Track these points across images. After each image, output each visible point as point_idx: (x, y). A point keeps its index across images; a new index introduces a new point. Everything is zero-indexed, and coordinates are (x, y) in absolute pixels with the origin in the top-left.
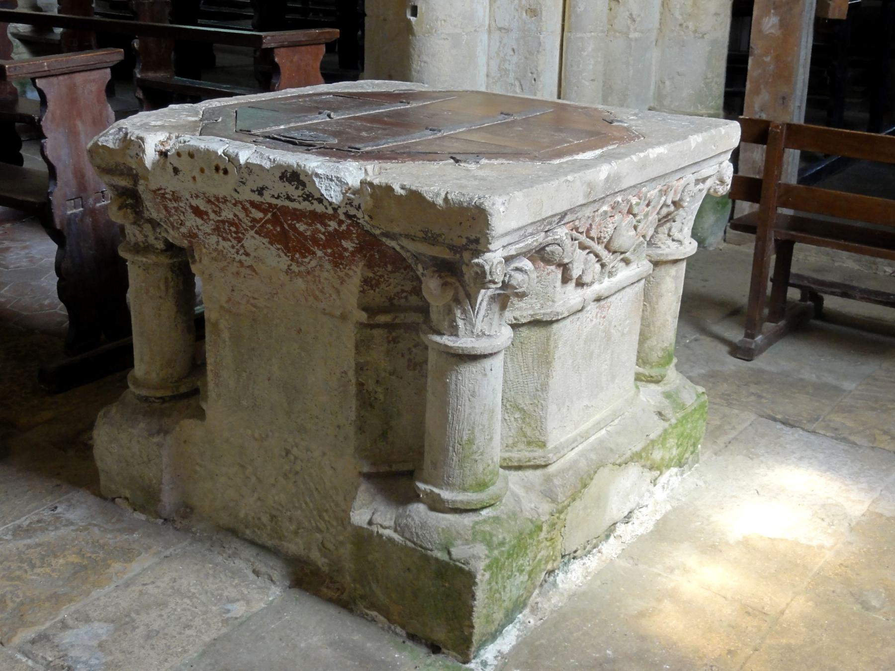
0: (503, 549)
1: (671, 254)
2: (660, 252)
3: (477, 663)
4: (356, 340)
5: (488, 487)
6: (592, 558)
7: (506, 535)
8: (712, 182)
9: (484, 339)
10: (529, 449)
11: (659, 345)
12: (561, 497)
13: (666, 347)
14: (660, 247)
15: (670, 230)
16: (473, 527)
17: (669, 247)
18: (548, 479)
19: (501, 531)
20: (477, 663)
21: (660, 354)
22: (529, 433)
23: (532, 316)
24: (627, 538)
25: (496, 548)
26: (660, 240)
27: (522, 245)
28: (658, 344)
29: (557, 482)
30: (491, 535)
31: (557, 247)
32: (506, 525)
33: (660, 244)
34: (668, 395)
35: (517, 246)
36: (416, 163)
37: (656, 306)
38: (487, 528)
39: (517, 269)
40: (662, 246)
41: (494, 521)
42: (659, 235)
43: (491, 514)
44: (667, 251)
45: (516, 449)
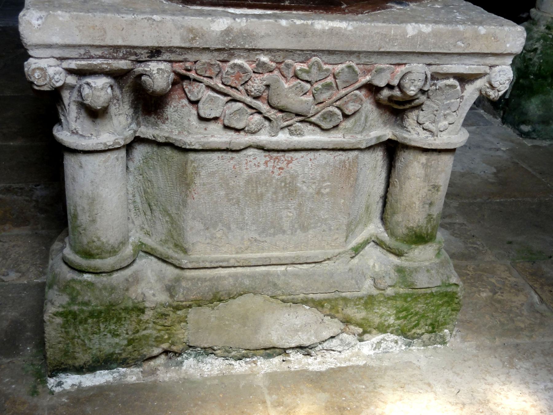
0: (85, 308)
1: (414, 141)
2: (406, 135)
3: (56, 381)
4: (453, 173)
5: (94, 258)
6: (244, 364)
7: (92, 299)
8: (482, 84)
9: (76, 137)
10: (176, 250)
11: (404, 223)
12: (180, 296)
13: (413, 227)
14: (410, 132)
15: (418, 116)
16: (69, 282)
17: (418, 134)
18: (178, 280)
19: (89, 294)
20: (56, 381)
21: (405, 231)
22: (175, 237)
23: (166, 138)
24: (295, 367)
25: (79, 304)
26: (410, 125)
27: (83, 62)
28: (403, 221)
29: (184, 284)
30: (78, 293)
31: (148, 78)
32: (97, 293)
33: (410, 128)
34: (400, 270)
35: (78, 62)
36: (334, 15)
37: (403, 186)
38: (78, 287)
39: (88, 84)
40: (412, 131)
41: (88, 285)
42: (409, 120)
43: (89, 279)
44: (415, 136)
45: (167, 246)
